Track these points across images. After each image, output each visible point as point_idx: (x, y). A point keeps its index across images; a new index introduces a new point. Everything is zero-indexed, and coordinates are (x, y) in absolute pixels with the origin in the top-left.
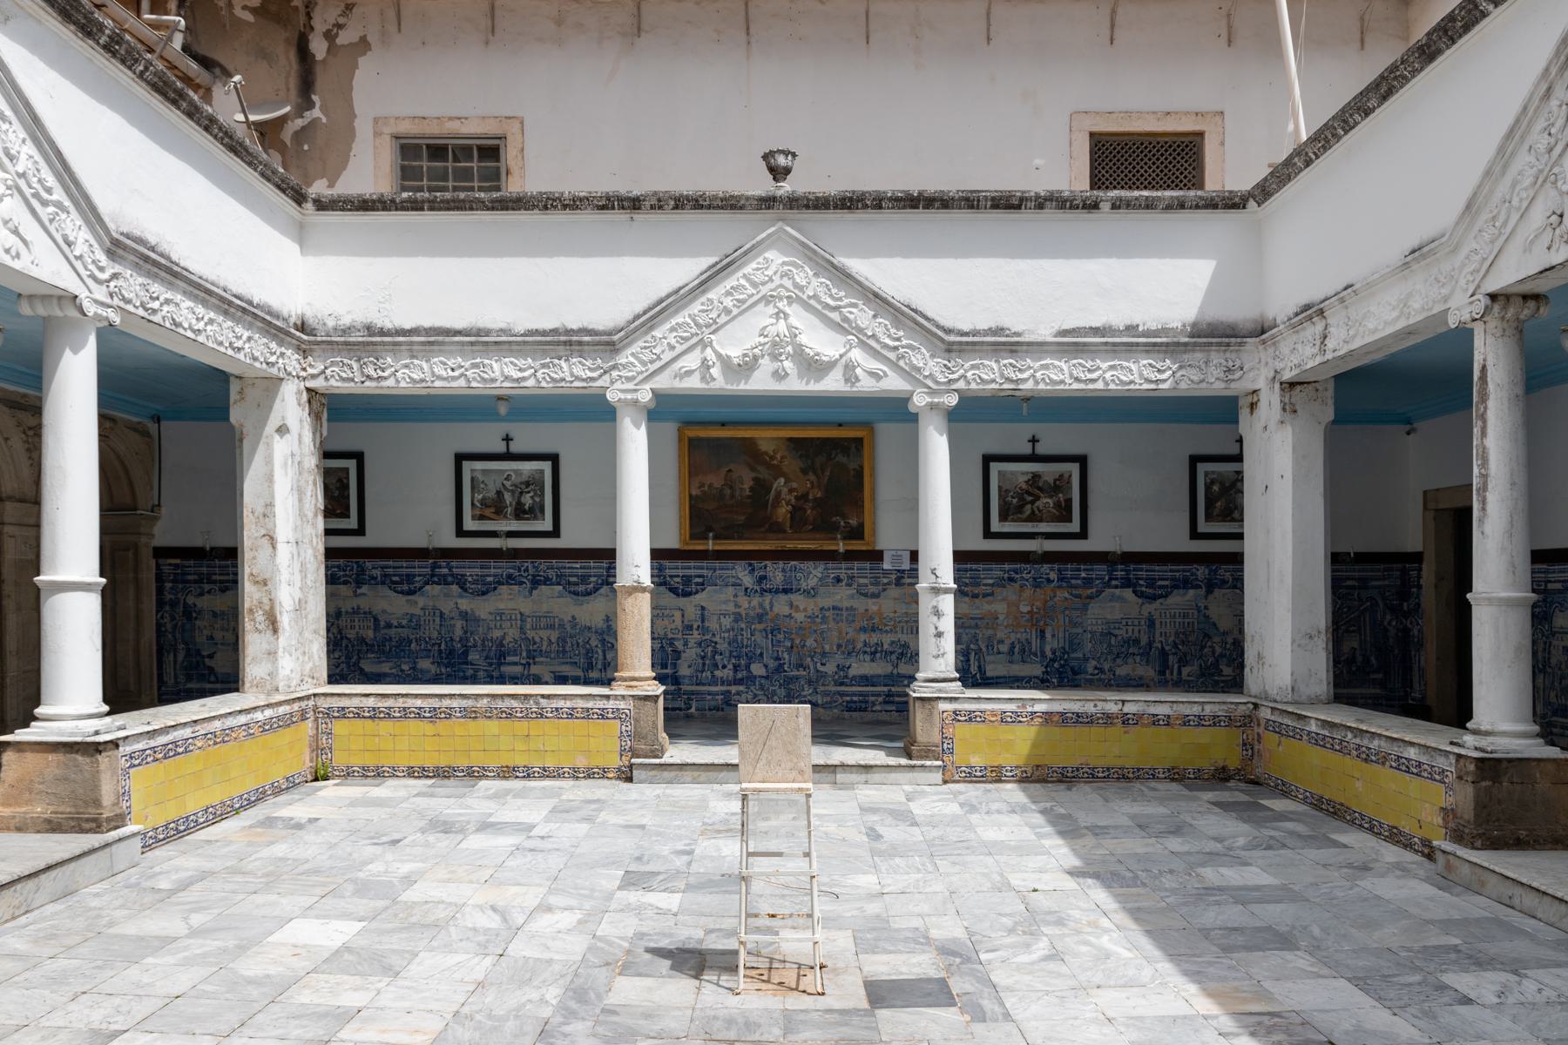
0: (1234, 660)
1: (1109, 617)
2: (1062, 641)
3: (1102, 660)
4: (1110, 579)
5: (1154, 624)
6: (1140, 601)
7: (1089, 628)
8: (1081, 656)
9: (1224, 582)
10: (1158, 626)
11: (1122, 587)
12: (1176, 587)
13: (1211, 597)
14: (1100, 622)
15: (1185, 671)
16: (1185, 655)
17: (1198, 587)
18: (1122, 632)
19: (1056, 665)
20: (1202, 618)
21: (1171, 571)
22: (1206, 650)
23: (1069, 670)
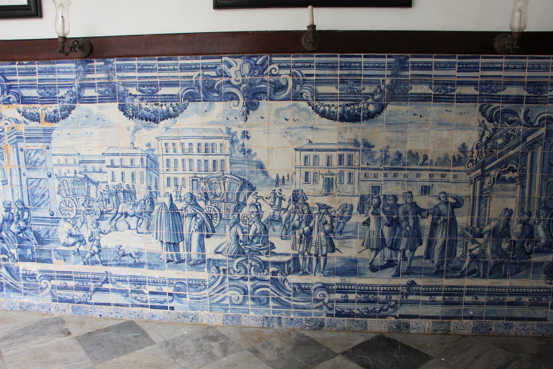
0: (295, 228)
1: (84, 152)
2: (17, 190)
3: (79, 224)
4: (82, 86)
5: (156, 163)
6: (132, 123)
7: (56, 171)
8: (48, 215)
9: (278, 88)
10: (162, 167)
11: (102, 101)
12: (192, 98)
13: (253, 115)
14: (70, 160)
15: (211, 244)
16: (210, 217)
17: (232, 97)
18: (106, 177)
19: (14, 228)
20: (238, 155)
21: (183, 68)
22: (246, 211)
23: (32, 236)
